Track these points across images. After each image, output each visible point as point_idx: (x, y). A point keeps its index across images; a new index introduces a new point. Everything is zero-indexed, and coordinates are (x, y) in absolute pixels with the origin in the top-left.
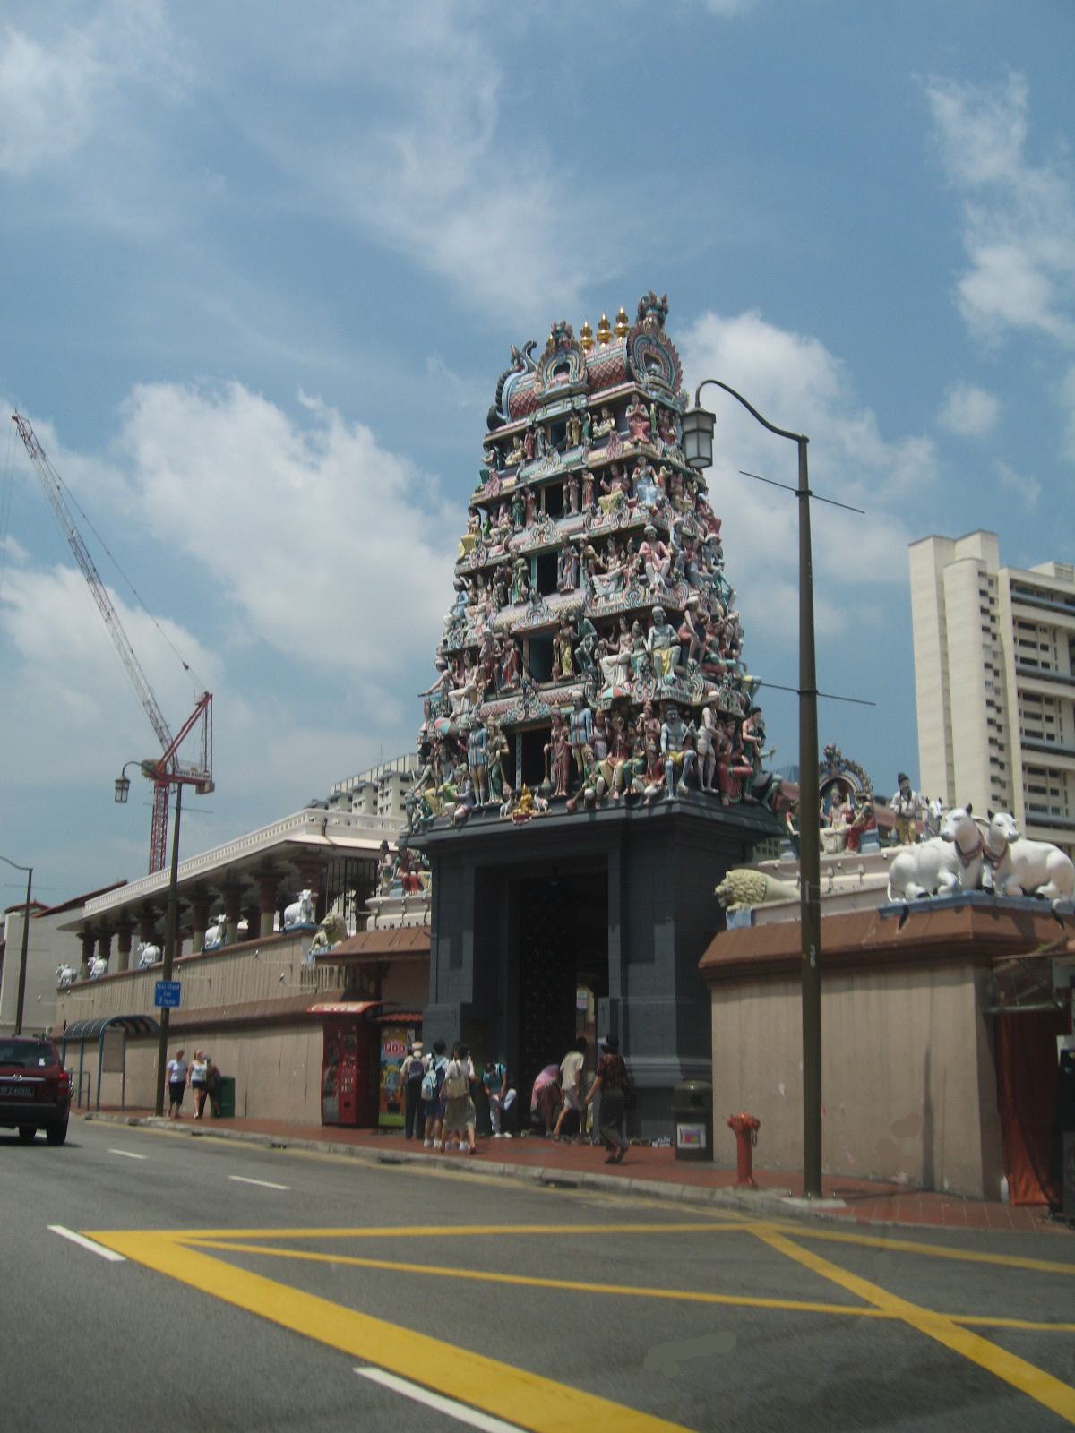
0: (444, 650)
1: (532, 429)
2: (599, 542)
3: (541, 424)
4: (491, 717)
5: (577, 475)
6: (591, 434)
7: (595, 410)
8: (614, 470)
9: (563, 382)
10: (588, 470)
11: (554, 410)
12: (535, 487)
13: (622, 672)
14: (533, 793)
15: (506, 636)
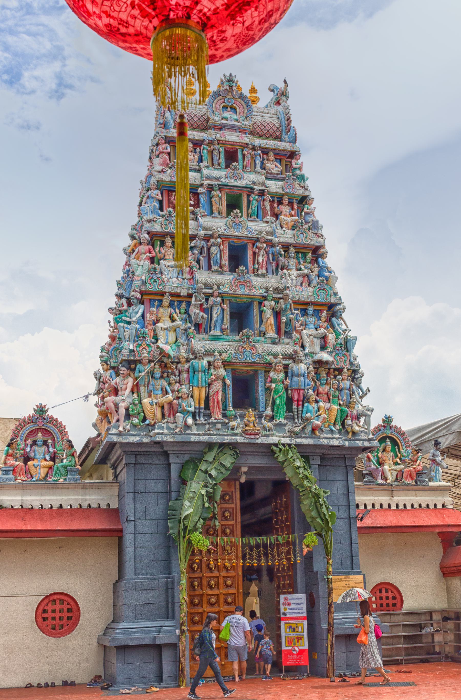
0: (144, 289)
1: (211, 143)
2: (286, 247)
3: (219, 142)
4: (216, 353)
5: (262, 193)
6: (263, 167)
7: (266, 151)
8: (286, 200)
9: (236, 120)
10: (269, 193)
11: (232, 137)
12: (221, 187)
13: (317, 343)
14: (260, 417)
15: (216, 294)
